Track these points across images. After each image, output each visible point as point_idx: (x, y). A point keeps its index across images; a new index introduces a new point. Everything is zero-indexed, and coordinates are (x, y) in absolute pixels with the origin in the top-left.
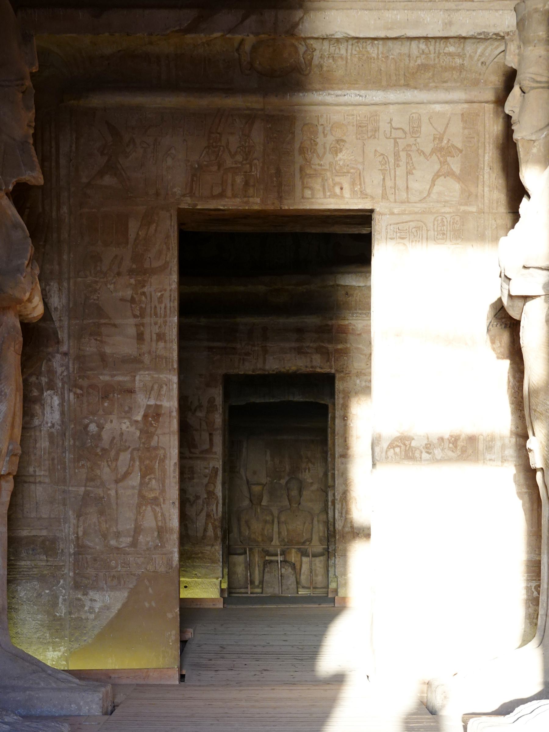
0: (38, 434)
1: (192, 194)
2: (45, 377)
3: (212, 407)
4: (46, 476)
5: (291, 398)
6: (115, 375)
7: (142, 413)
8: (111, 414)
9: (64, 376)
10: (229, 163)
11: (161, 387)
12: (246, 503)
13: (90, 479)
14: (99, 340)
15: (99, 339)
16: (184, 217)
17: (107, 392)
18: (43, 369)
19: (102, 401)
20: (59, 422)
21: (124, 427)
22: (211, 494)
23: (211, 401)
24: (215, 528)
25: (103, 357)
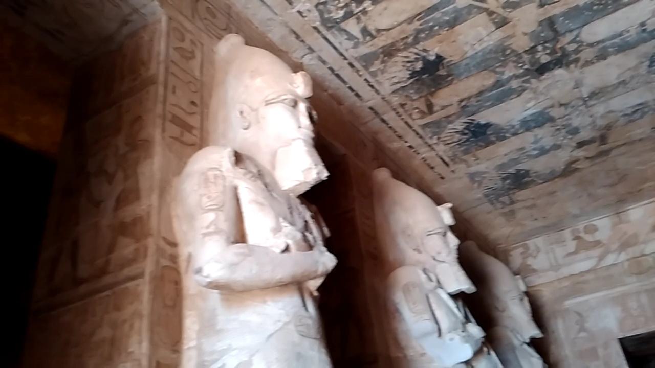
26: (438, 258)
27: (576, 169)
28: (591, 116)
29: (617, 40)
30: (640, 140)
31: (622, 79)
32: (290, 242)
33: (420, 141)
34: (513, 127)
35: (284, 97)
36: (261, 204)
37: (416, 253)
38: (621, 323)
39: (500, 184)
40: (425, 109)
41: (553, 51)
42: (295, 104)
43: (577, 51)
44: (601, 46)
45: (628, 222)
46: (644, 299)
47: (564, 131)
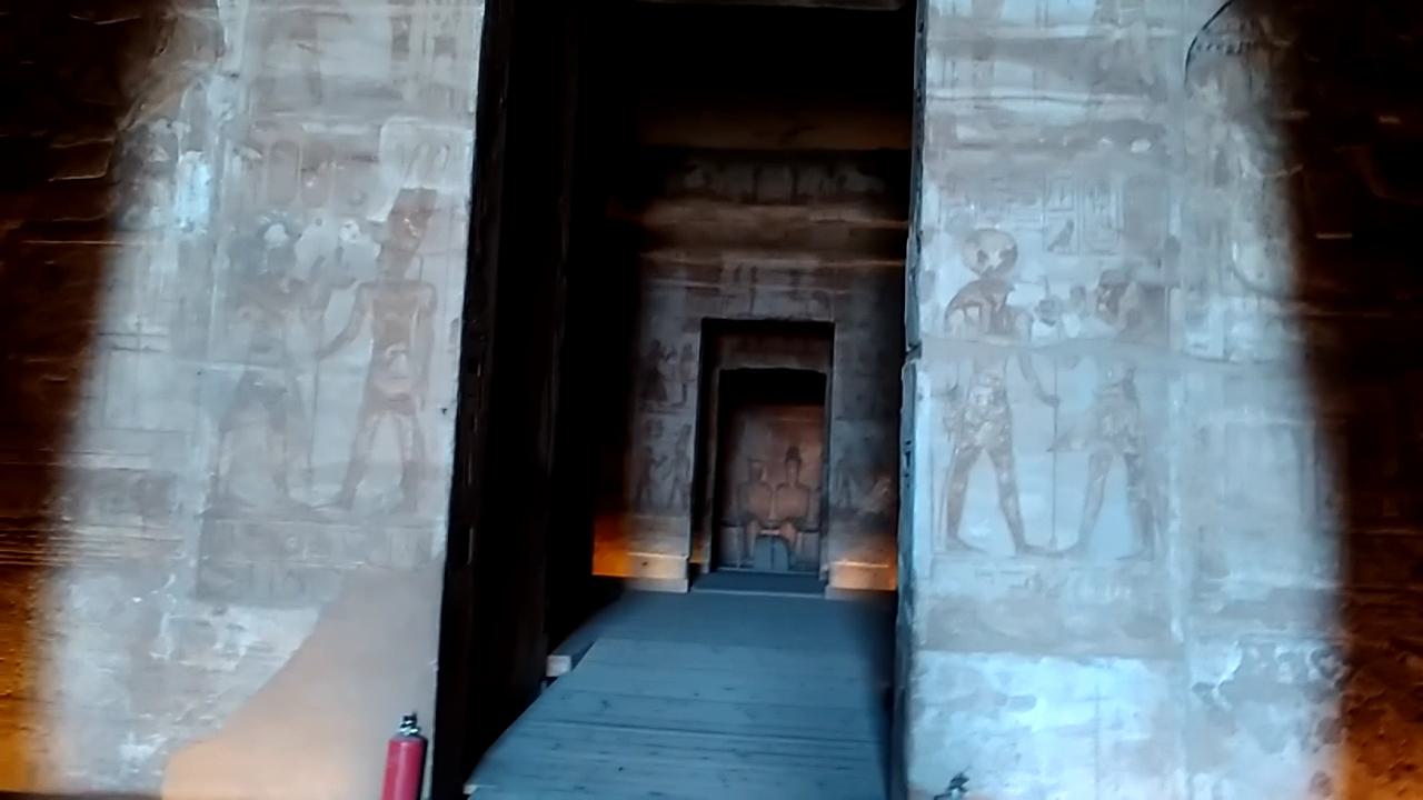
0: (154, 242)
2: (185, 122)
3: (687, 356)
4: (163, 336)
5: (787, 366)
6: (337, 123)
7: (389, 207)
8: (319, 205)
9: (227, 122)
11: (434, 152)
12: (746, 478)
13: (261, 348)
14: (308, 48)
15: (308, 45)
17: (314, 160)
18: (182, 106)
19: (302, 177)
20: (206, 221)
21: (346, 236)
22: (681, 454)
23: (688, 348)
24: (684, 496)
25: (314, 84)
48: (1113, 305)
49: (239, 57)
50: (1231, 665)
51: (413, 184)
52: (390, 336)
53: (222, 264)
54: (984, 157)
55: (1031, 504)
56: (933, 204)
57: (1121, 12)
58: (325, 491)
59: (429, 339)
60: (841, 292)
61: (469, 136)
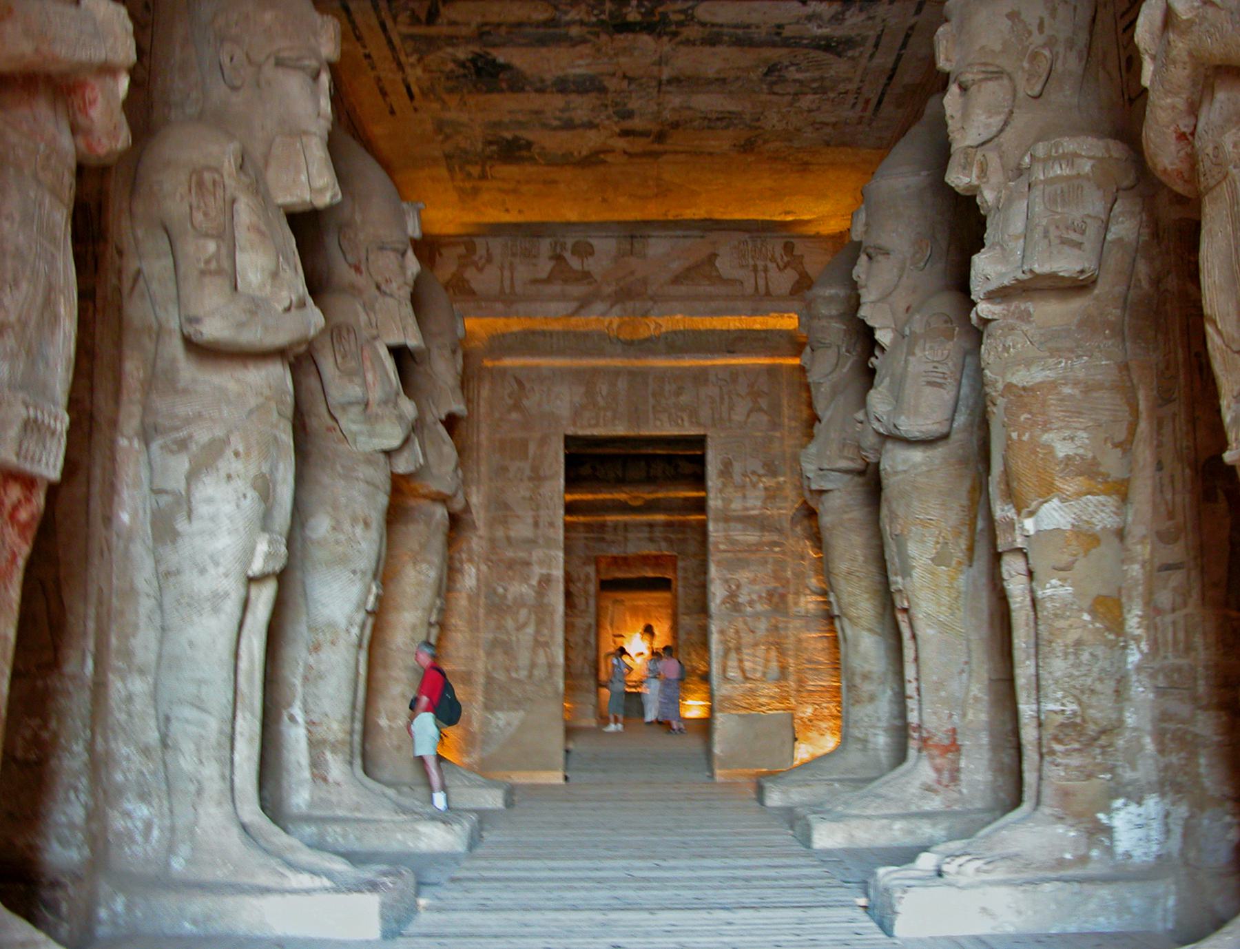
1: (574, 424)
10: (602, 403)
16: (569, 440)
17: (511, 564)
23: (587, 576)
25: (508, 539)
26: (383, 287)
27: (604, 162)
28: (659, 104)
29: (740, 32)
30: (711, 154)
31: (722, 75)
32: (294, 298)
33: (388, 53)
34: (542, 81)
35: (307, 62)
36: (262, 233)
37: (353, 272)
38: (576, 414)
39: (480, 146)
40: (423, 17)
41: (651, 12)
42: (316, 77)
43: (680, 24)
44: (715, 29)
45: (645, 256)
46: (622, 384)
47: (611, 110)
48: (770, 600)
49: (482, 530)
50: (809, 711)
51: (544, 571)
52: (540, 622)
53: (482, 601)
54: (729, 555)
55: (747, 665)
56: (713, 570)
57: (769, 506)
58: (523, 674)
59: (553, 622)
60: (680, 536)
61: (561, 554)
